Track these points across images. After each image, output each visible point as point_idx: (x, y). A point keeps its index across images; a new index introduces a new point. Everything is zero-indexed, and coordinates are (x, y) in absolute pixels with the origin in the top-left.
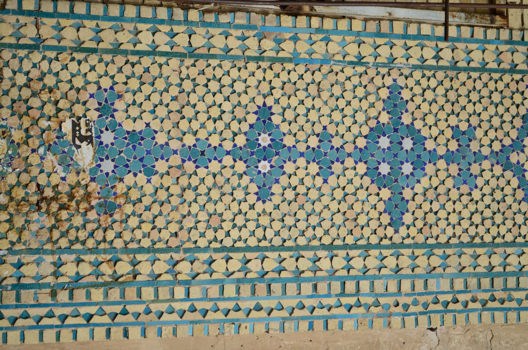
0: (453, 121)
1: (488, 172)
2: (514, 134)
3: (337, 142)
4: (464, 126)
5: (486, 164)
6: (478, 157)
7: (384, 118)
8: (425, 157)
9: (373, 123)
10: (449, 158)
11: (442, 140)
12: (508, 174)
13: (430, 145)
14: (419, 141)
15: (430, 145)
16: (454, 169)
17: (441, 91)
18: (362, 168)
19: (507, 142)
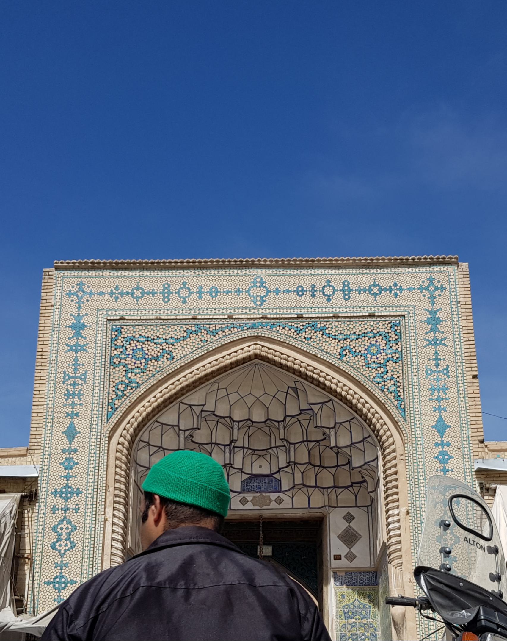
0: (53, 568)
1: (66, 559)
2: (57, 552)
3: (56, 597)
4: (54, 565)
5: (64, 559)
6: (62, 561)
7: (51, 585)
8: (61, 575)
9: (52, 588)
10: (61, 569)
11: (57, 571)
12: (66, 553)
13: (58, 574)
14: (57, 577)
15: (58, 574)
16: (64, 568)
17: (46, 571)
18: (62, 591)
19: (59, 554)
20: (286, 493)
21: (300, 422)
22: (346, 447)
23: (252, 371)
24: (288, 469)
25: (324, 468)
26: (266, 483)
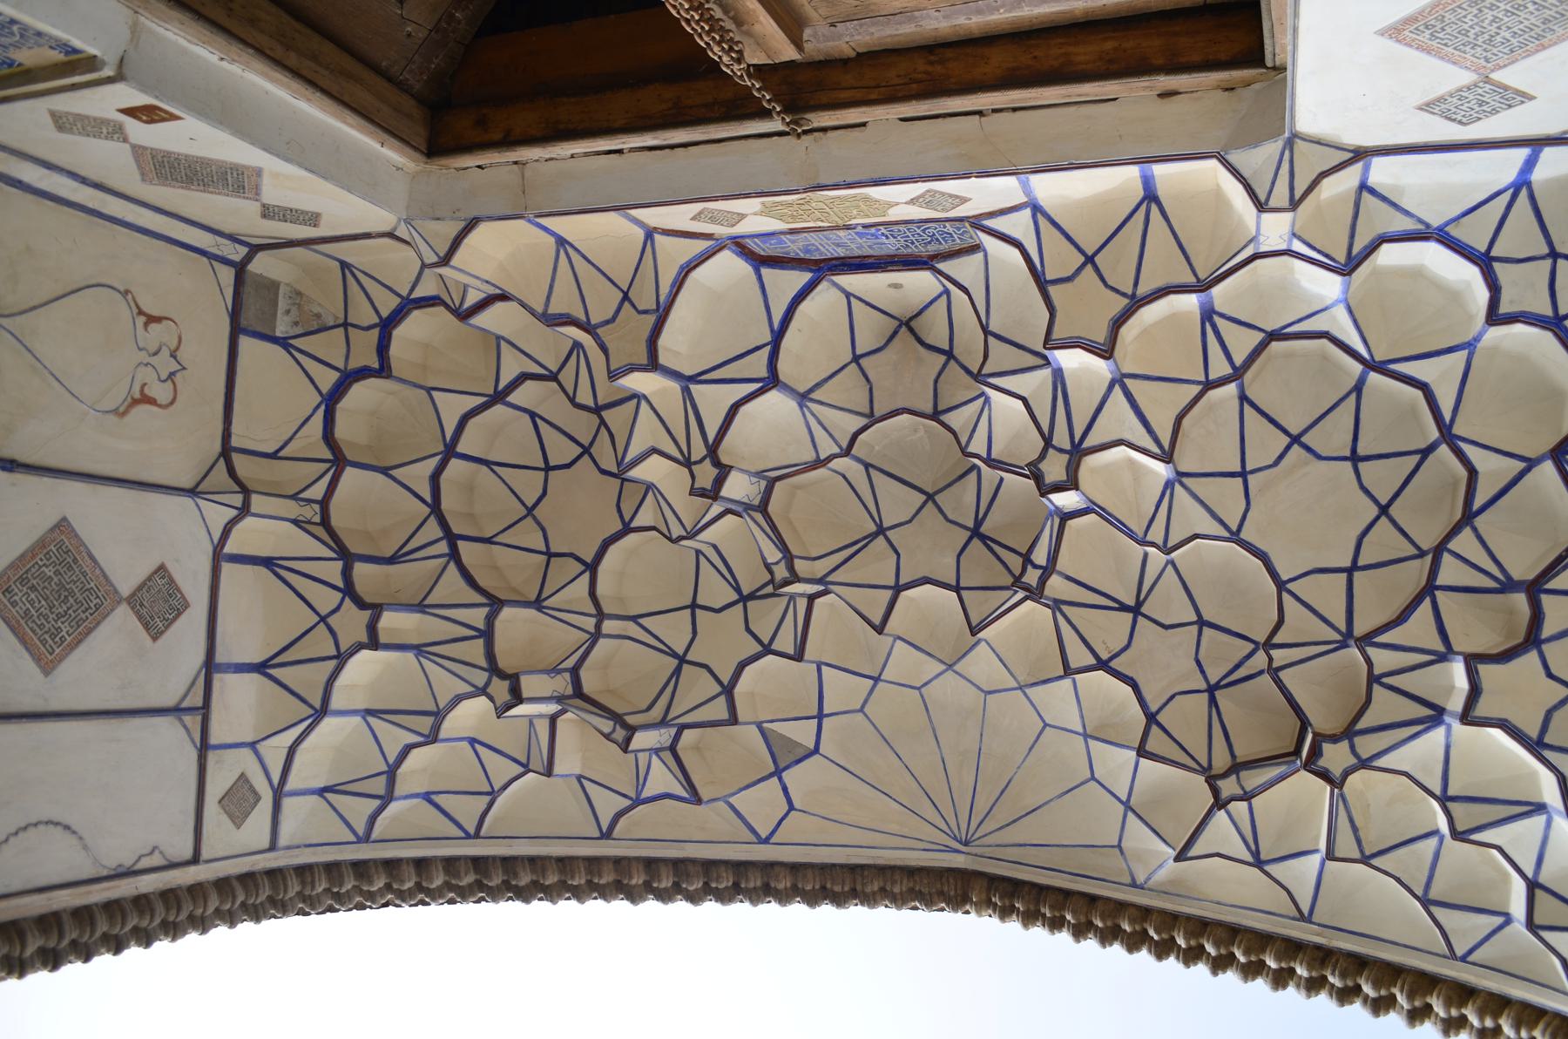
20: (702, 245)
21: (738, 589)
22: (458, 699)
23: (982, 806)
24: (714, 400)
25: (553, 377)
26: (838, 245)
